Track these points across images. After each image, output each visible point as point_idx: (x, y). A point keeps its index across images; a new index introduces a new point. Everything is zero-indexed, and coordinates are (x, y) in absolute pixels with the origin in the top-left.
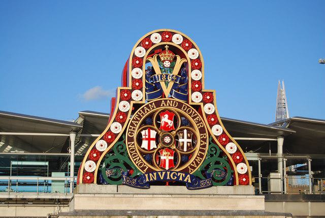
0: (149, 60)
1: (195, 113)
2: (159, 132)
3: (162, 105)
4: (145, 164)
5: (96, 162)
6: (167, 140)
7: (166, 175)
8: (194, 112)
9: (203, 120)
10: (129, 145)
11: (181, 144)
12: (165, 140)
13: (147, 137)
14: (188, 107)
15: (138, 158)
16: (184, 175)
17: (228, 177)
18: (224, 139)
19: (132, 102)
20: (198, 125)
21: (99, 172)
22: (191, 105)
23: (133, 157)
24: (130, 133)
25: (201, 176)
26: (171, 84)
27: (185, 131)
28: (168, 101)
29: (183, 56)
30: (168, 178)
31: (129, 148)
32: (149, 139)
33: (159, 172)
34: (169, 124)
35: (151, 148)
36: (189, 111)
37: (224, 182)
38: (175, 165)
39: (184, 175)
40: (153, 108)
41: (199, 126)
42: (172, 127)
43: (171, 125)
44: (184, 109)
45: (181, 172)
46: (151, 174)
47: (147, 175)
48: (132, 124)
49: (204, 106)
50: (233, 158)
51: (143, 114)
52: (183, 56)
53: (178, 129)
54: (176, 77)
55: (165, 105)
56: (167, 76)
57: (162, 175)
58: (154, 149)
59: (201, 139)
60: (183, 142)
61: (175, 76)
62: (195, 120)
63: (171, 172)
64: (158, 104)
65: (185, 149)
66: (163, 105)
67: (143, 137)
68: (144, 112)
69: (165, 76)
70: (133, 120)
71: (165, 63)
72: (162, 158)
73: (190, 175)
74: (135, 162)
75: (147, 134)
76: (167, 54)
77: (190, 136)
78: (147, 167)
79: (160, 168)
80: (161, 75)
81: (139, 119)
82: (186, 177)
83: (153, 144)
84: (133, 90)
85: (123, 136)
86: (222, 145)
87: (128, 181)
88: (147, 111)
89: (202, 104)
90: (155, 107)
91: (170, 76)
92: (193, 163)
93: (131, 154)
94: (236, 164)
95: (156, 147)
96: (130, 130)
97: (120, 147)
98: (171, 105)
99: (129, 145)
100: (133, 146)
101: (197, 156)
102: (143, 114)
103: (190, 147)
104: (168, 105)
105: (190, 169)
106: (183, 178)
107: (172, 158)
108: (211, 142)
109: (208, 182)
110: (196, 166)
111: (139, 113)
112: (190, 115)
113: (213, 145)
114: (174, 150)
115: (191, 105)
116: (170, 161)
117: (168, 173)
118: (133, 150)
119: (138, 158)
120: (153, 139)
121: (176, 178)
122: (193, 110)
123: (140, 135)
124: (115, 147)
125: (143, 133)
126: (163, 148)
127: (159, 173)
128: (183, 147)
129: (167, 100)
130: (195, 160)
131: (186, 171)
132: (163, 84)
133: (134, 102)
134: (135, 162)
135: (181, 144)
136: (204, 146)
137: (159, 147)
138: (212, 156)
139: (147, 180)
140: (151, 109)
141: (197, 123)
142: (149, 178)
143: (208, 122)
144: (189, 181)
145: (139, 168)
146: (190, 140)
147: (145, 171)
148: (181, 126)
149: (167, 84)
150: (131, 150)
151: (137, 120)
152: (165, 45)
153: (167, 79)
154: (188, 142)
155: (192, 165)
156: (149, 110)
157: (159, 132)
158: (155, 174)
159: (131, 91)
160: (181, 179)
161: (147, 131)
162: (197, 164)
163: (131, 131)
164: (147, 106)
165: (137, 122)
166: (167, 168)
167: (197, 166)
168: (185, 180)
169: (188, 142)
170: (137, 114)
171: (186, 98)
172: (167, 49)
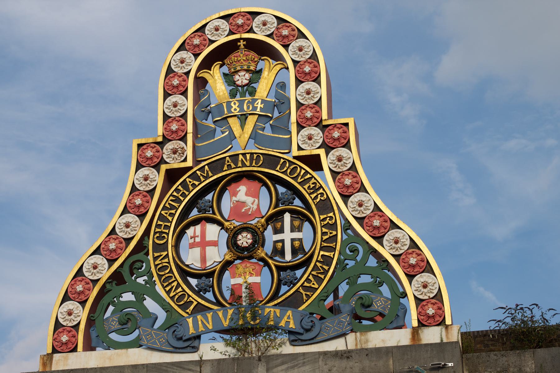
0: (206, 76)
1: (307, 172)
5: (83, 303)
9: (324, 186)
10: (155, 259)
11: (280, 245)
13: (198, 240)
14: (291, 163)
18: (376, 223)
19: (164, 167)
21: (90, 322)
23: (165, 284)
27: (287, 217)
29: (275, 56)
31: (156, 266)
32: (204, 244)
36: (293, 171)
39: (278, 311)
43: (255, 207)
47: (190, 321)
49: (327, 154)
52: (275, 56)
57: (225, 316)
60: (282, 241)
61: (260, 101)
62: (306, 187)
65: (288, 256)
69: (237, 105)
70: (164, 208)
71: (237, 77)
75: (198, 232)
78: (195, 303)
84: (166, 140)
85: (146, 238)
86: (374, 238)
89: (322, 152)
91: (249, 102)
93: (160, 276)
96: (157, 230)
98: (248, 164)
100: (166, 260)
112: (295, 179)
118: (163, 268)
122: (301, 167)
124: (126, 268)
127: (220, 314)
128: (282, 253)
141: (309, 194)
143: (338, 187)
145: (176, 307)
150: (161, 269)
152: (238, 40)
154: (293, 240)
159: (161, 144)
161: (198, 228)
165: (173, 211)
169: (293, 240)
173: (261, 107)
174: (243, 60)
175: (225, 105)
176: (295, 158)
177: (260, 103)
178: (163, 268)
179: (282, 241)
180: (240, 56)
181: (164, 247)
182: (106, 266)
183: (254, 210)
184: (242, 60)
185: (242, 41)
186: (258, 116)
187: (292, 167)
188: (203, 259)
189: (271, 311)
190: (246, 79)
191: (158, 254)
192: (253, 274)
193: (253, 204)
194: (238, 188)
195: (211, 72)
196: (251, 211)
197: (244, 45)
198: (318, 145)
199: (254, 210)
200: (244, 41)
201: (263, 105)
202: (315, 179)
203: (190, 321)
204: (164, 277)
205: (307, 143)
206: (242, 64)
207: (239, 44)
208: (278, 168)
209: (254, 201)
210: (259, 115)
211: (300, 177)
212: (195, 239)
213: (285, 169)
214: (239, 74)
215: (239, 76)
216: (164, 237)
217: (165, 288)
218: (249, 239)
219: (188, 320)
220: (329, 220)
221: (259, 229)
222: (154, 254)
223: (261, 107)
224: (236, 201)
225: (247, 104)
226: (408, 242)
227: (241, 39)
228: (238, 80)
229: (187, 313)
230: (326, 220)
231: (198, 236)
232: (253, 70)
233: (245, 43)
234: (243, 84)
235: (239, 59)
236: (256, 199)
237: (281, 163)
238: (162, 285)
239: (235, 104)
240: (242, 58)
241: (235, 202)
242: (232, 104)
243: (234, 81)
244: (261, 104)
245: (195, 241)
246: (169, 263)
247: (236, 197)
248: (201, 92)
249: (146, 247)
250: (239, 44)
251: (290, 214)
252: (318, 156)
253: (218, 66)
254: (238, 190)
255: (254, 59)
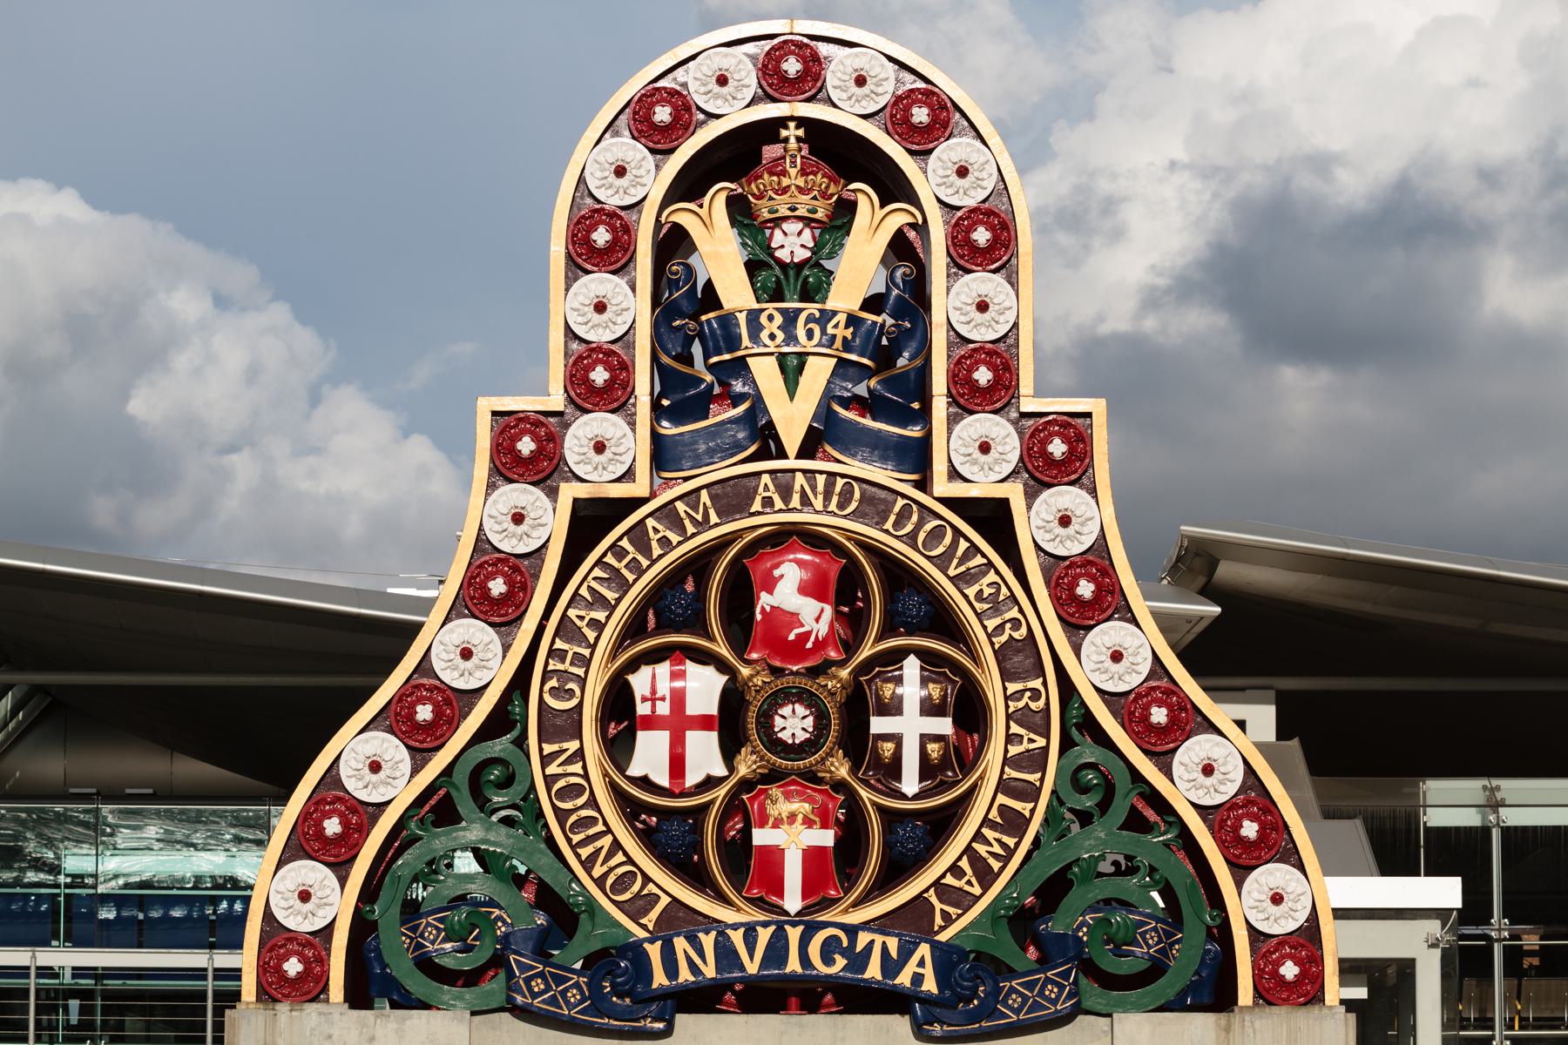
1: (974, 549)
2: (745, 671)
3: (757, 506)
4: (647, 879)
5: (341, 869)
6: (794, 723)
7: (777, 951)
8: (963, 545)
10: (546, 760)
12: (778, 721)
13: (663, 709)
15: (606, 841)
16: (893, 944)
17: (1187, 956)
19: (569, 492)
20: (991, 624)
21: (362, 927)
22: (942, 500)
24: (553, 683)
25: (1005, 947)
26: (818, 372)
28: (800, 479)
29: (894, 187)
30: (794, 965)
31: (549, 780)
32: (679, 723)
33: (735, 927)
34: (809, 623)
35: (692, 778)
36: (936, 535)
37: (1167, 986)
38: (849, 881)
40: (704, 525)
41: (1000, 628)
42: (820, 645)
43: (822, 629)
44: (897, 525)
45: (881, 924)
46: (680, 944)
48: (566, 629)
50: (1216, 831)
51: (635, 566)
52: (894, 187)
53: (866, 652)
54: (852, 320)
55: (779, 504)
56: (790, 318)
58: (710, 783)
59: (1009, 717)
60: (897, 739)
61: (842, 318)
62: (971, 592)
63: (811, 929)
64: (733, 497)
65: (910, 783)
66: (768, 502)
67: (643, 709)
68: (646, 551)
69: (779, 320)
72: (761, 837)
73: (935, 946)
74: (589, 873)
76: (794, 178)
77: (944, 697)
79: (751, 901)
80: (753, 316)
81: (611, 595)
82: (906, 953)
83: (704, 755)
85: (516, 696)
87: (537, 985)
88: (664, 541)
89: (1014, 493)
90: (714, 519)
91: (811, 318)
92: (955, 869)
94: (1241, 871)
95: (720, 770)
97: (495, 773)
99: (546, 760)
100: (577, 768)
101: (986, 822)
102: (635, 566)
103: (945, 763)
104: (795, 502)
105: (938, 906)
106: (891, 967)
107: (826, 838)
108: (1075, 733)
109: (1051, 991)
110: (977, 890)
111: (610, 559)
112: (942, 562)
113: (1088, 752)
114: (840, 786)
115: (946, 502)
116: (813, 856)
117: (794, 934)
119: (606, 841)
120: (704, 723)
121: (841, 962)
122: (958, 532)
123: (618, 701)
124: (461, 776)
125: (639, 682)
126: (772, 776)
127: (737, 937)
128: (894, 769)
129: (793, 471)
130: (969, 850)
131: (913, 919)
132: (765, 372)
133: (582, 491)
134: (588, 864)
135: (888, 748)
136: (1037, 761)
137: (743, 770)
138: (1085, 818)
139: (660, 979)
140: (690, 529)
142: (671, 969)
144: (930, 985)
146: (944, 726)
147: (650, 919)
148: (887, 631)
149: (792, 369)
151: (599, 600)
152: (782, 122)
153: (791, 338)
154: (925, 739)
155: (949, 880)
156: (675, 538)
157: (745, 671)
158: (708, 941)
160: (873, 971)
162: (986, 876)
163: (563, 675)
164: (667, 513)
166: (793, 901)
167: (985, 890)
168: (904, 979)
169: (925, 739)
170: (599, 562)
171: (916, 458)
172: (793, 144)
173: (845, 338)
174: (798, 187)
175: (742, 318)
176: (942, 500)
177: (842, 325)
178: (572, 791)
179: (897, 739)
180: (784, 173)
181: (571, 725)
182: (406, 766)
183: (821, 639)
184: (793, 188)
185: (792, 125)
186: (836, 360)
187: (929, 527)
188: (677, 765)
189: (872, 942)
190: (802, 246)
191: (555, 747)
192: (815, 822)
193: (817, 620)
194: (777, 566)
195: (703, 212)
196: (812, 638)
197: (798, 139)
198: (1007, 469)
199: (821, 639)
200: (797, 127)
201: (851, 329)
202: (998, 573)
203: (654, 951)
204: (573, 818)
205: (975, 462)
206: (794, 200)
207: (784, 133)
208: (889, 525)
209: (822, 610)
210: (840, 359)
211: (955, 561)
212: (654, 706)
213: (909, 528)
214: (785, 226)
215: (785, 234)
216: (571, 693)
217: (579, 850)
218: (804, 718)
219: (646, 945)
220: (1029, 698)
221: (832, 694)
222: (544, 745)
223: (845, 338)
224: (772, 607)
225: (805, 325)
226: (1238, 775)
227: (792, 118)
228: (782, 246)
229: (644, 927)
230: (1023, 696)
231: (663, 699)
232: (825, 219)
233: (801, 132)
234: (796, 260)
235: (785, 182)
236: (825, 605)
237: (897, 509)
238: (569, 840)
239: (771, 318)
240: (793, 182)
241: (768, 609)
242: (763, 319)
243: (769, 247)
244: (847, 327)
245: (653, 711)
246: (586, 776)
247: (771, 592)
248: (674, 268)
249: (516, 721)
250: (784, 133)
251: (919, 662)
252: (1004, 504)
253: (722, 197)
254: (777, 573)
255: (827, 187)
